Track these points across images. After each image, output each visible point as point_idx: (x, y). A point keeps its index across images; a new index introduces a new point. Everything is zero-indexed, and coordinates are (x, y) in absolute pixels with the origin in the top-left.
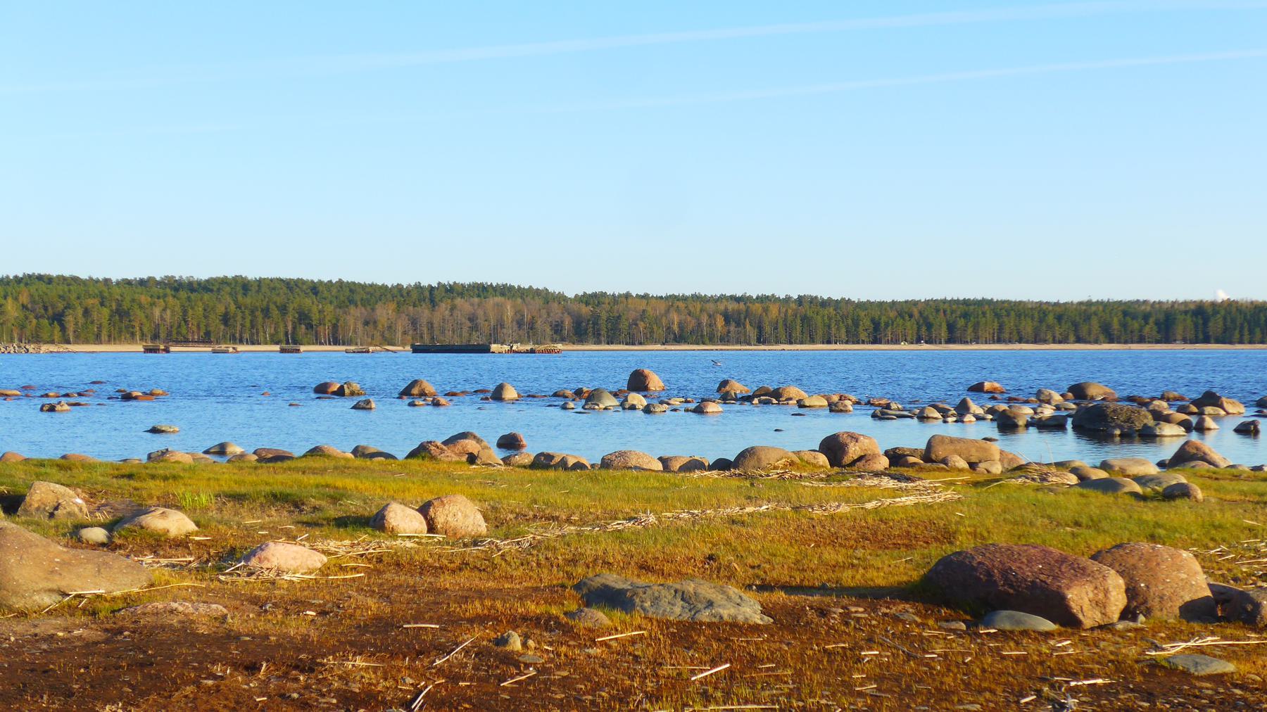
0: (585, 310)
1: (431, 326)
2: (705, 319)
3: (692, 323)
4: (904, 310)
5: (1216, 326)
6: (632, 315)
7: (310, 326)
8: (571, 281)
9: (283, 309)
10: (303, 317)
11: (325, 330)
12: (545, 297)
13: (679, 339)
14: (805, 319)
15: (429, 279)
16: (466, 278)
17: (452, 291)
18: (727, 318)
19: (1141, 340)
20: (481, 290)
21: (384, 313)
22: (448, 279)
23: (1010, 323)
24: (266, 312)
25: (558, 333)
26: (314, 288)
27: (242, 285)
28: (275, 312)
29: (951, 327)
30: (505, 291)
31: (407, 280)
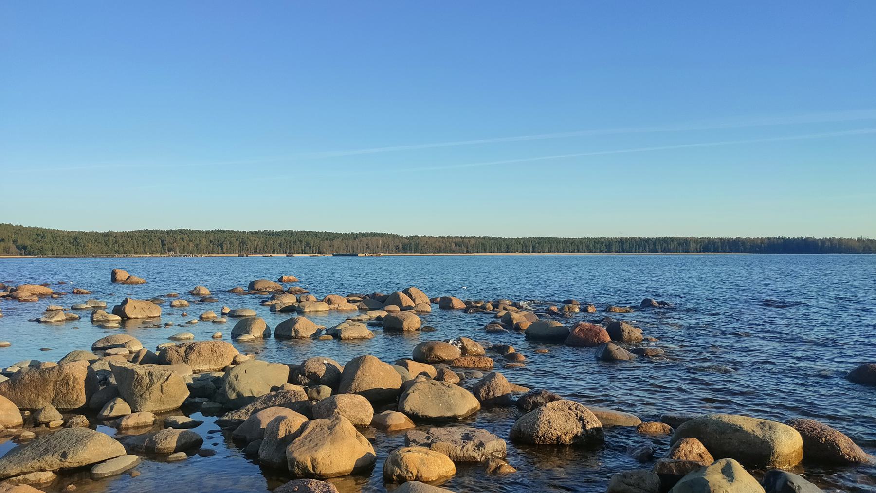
0: (407, 241)
1: (353, 247)
2: (448, 245)
3: (443, 246)
4: (518, 241)
5: (626, 246)
6: (423, 243)
9: (301, 242)
10: (308, 244)
11: (315, 249)
13: (439, 251)
14: (483, 244)
19: (600, 251)
21: (337, 243)
23: (554, 246)
24: (295, 242)
25: (397, 250)
28: (298, 243)
29: (534, 247)
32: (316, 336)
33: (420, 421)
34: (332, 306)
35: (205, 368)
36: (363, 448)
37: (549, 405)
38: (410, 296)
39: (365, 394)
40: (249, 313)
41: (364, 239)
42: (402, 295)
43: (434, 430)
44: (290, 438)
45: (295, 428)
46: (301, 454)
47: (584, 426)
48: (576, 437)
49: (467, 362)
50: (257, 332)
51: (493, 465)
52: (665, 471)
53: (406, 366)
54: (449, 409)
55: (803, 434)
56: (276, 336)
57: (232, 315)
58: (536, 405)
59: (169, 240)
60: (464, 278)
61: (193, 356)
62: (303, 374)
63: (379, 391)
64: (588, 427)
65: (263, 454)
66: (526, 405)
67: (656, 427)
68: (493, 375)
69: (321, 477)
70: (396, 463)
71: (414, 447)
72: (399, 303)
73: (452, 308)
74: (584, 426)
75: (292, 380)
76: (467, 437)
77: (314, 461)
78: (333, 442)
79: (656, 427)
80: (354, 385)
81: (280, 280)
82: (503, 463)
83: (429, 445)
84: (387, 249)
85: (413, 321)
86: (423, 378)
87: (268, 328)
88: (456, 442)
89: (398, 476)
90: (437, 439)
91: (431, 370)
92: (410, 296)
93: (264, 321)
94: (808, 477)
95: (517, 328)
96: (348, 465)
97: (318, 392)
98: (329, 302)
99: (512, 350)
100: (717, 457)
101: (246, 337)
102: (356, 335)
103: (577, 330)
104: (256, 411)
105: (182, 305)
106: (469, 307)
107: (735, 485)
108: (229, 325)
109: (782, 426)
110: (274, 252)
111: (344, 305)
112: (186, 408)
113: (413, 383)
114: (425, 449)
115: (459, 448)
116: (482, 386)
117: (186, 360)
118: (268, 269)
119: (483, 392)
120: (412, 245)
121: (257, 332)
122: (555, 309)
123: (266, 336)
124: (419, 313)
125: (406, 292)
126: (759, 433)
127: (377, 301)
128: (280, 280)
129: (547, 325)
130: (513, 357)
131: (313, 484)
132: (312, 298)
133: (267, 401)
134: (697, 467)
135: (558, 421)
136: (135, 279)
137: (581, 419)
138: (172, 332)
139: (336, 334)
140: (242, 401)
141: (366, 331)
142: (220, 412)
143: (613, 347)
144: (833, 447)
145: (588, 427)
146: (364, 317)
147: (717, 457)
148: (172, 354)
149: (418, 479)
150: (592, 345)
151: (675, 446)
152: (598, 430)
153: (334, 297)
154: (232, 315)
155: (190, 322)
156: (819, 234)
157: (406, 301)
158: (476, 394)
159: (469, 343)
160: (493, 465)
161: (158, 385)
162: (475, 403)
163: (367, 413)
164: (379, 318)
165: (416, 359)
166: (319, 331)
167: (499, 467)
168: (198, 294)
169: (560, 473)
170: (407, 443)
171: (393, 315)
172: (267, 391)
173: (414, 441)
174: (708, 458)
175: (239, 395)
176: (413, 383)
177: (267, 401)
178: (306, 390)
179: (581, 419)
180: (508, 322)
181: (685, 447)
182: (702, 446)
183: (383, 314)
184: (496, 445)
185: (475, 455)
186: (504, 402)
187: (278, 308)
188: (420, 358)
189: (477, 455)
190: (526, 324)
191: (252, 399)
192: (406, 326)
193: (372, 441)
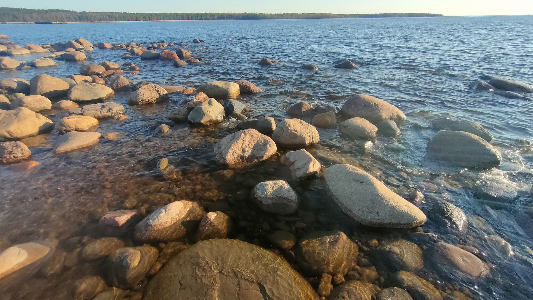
0: (80, 15)
7: (17, 18)
12: (72, 12)
13: (101, 20)
14: (123, 16)
15: (46, 8)
16: (54, 8)
18: (109, 16)
22: (50, 8)
25: (76, 20)
31: (40, 8)
32: (19, 68)
33: (81, 103)
34: (32, 51)
36: (44, 120)
38: (81, 44)
47: (160, 94)
48: (157, 99)
49: (109, 72)
52: (190, 107)
54: (96, 95)
55: (240, 86)
60: (112, 33)
64: (161, 94)
66: (135, 88)
70: (62, 125)
71: (73, 116)
72: (74, 47)
74: (160, 94)
77: (8, 132)
83: (82, 114)
84: (69, 19)
85: (81, 56)
88: (97, 110)
89: (66, 130)
91: (89, 78)
92: (81, 44)
95: (137, 55)
98: (29, 48)
99: (133, 65)
103: (163, 54)
106: (114, 47)
111: (40, 49)
116: (114, 83)
119: (114, 85)
120: (83, 17)
125: (77, 41)
126: (224, 87)
127: (61, 47)
129: (150, 53)
130: (133, 69)
134: (201, 103)
135: (148, 93)
139: (33, 65)
141: (52, 62)
145: (161, 94)
146: (53, 55)
152: (166, 95)
153: (32, 46)
157: (78, 46)
158: (111, 86)
160: (116, 117)
162: (110, 91)
163: (48, 104)
164: (61, 55)
165: (82, 74)
166: (22, 65)
167: (119, 117)
170: (70, 114)
171: (68, 53)
179: (158, 91)
180: (133, 52)
182: (205, 95)
184: (117, 108)
189: (109, 114)
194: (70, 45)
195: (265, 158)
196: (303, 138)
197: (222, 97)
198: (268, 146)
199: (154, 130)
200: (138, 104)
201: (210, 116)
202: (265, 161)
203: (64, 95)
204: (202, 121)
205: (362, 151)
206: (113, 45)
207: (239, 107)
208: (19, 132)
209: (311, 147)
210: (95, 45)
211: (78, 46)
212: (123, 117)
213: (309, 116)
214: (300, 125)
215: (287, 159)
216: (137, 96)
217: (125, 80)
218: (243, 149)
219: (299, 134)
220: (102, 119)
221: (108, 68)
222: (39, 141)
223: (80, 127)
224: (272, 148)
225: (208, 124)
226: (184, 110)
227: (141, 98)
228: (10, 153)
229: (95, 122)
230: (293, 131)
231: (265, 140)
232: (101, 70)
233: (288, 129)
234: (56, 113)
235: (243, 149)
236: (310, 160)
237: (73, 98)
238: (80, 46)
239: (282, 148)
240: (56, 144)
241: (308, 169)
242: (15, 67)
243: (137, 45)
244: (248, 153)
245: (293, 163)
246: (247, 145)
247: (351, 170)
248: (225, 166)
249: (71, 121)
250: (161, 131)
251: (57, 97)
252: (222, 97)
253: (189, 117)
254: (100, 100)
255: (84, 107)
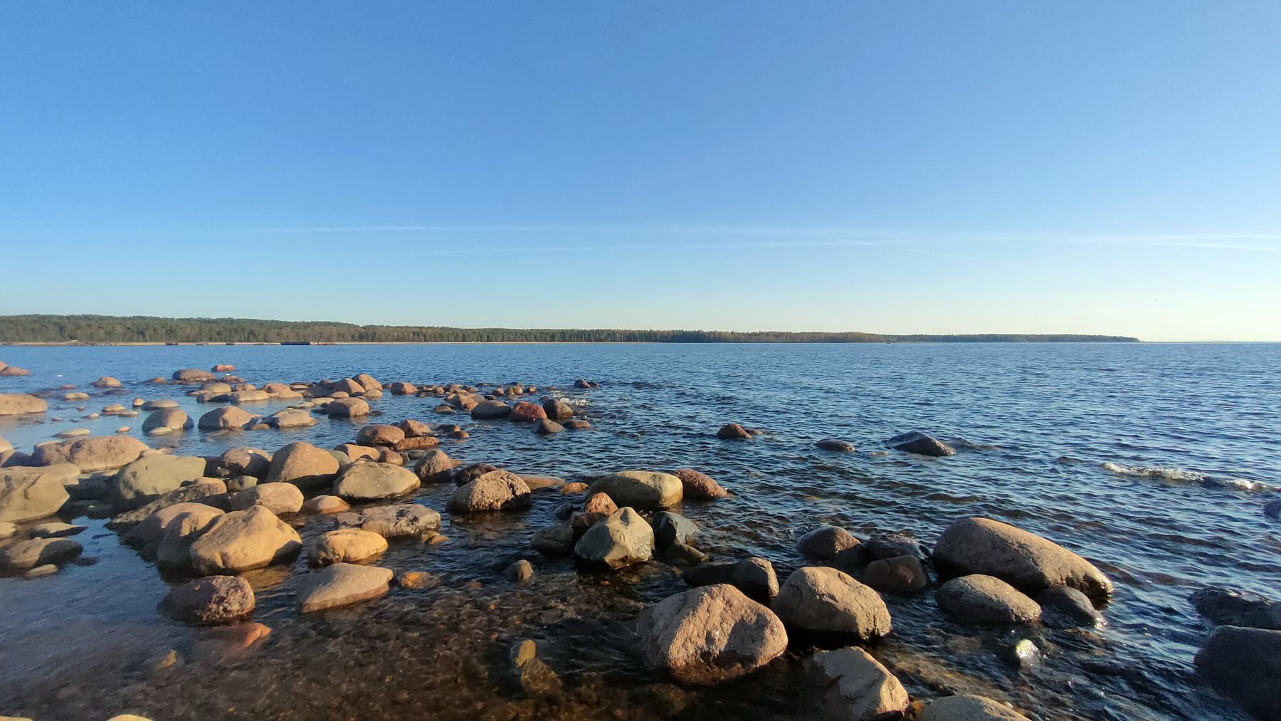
4: (474, 332)
5: (567, 337)
8: (362, 320)
10: (252, 333)
17: (315, 324)
20: (328, 324)
21: (285, 332)
25: (353, 338)
26: (261, 323)
27: (232, 321)
30: (336, 324)
32: (248, 427)
33: (355, 502)
35: (99, 466)
36: (289, 535)
37: (483, 476)
38: (361, 383)
39: (294, 482)
40: (167, 404)
41: (316, 328)
42: (350, 381)
43: (368, 511)
44: (196, 535)
45: (203, 523)
46: (208, 551)
47: (514, 493)
50: (175, 424)
51: (425, 537)
53: (345, 450)
54: (387, 488)
56: (200, 427)
57: (146, 407)
58: (474, 477)
59: (70, 327)
61: (81, 455)
62: (223, 466)
63: (313, 478)
64: (518, 493)
65: (162, 555)
66: (464, 477)
67: (576, 486)
68: (434, 453)
69: (236, 572)
70: (322, 547)
71: (343, 530)
73: (404, 393)
74: (514, 493)
75: (209, 472)
76: (401, 514)
78: (248, 534)
79: (576, 486)
80: (284, 473)
81: (215, 370)
82: (435, 534)
83: (360, 526)
84: (342, 337)
85: (360, 407)
86: (362, 462)
87: (189, 420)
89: (324, 560)
90: (371, 518)
91: (373, 452)
93: (182, 411)
94: (685, 514)
96: (268, 555)
97: (241, 483)
98: (269, 390)
99: (458, 429)
100: (619, 506)
101: (161, 431)
102: (295, 422)
104: (159, 508)
105: (79, 399)
106: (421, 391)
107: (630, 527)
108: (141, 417)
109: (668, 476)
110: (210, 340)
111: (287, 392)
112: (65, 514)
113: (350, 466)
114: (354, 530)
115: (392, 525)
116: (423, 464)
117: (71, 459)
118: (197, 359)
119: (423, 470)
120: (368, 334)
121: (175, 424)
122: (501, 391)
123: (188, 427)
124: (369, 399)
125: (356, 379)
126: (651, 484)
127: (326, 389)
128: (215, 370)
129: (492, 405)
130: (458, 436)
131: (219, 581)
132: (250, 387)
133: (174, 497)
134: (603, 517)
135: (491, 489)
136: (15, 370)
137: (511, 486)
138: (57, 428)
139: (273, 423)
140: (142, 500)
141: (306, 418)
142: (114, 514)
143: (548, 422)
144: (703, 489)
145: (518, 493)
146: (308, 404)
147: (619, 506)
148: (51, 454)
149: (346, 560)
150: (529, 421)
151: (588, 500)
152: (527, 494)
154: (146, 407)
155: (87, 417)
156: (706, 328)
157: (356, 387)
159: (414, 425)
160: (425, 537)
161: (20, 490)
162: (414, 480)
163: (296, 500)
164: (324, 405)
165: (360, 444)
166: (253, 421)
167: (431, 539)
168: (105, 386)
169: (489, 535)
170: (337, 525)
172: (175, 486)
173: (344, 523)
174: (614, 507)
175: (138, 493)
176: (350, 466)
177: (174, 497)
178: (226, 482)
179: (511, 486)
180: (457, 404)
181: (595, 501)
183: (329, 401)
184: (429, 517)
185: (409, 529)
186: (444, 478)
187: (207, 398)
188: (364, 441)
189: (411, 530)
190: (473, 405)
191: (155, 498)
192: (352, 411)
193: (297, 528)
194: (343, 386)
195: (762, 661)
196: (850, 620)
197: (649, 504)
198: (768, 632)
199: (503, 570)
200: (468, 512)
201: (624, 547)
202: (762, 668)
203: (327, 484)
204: (607, 559)
205: (1012, 663)
206: (420, 388)
207: (685, 528)
208: (242, 556)
209: (875, 642)
210: (384, 387)
211: (356, 387)
212: (438, 537)
213: (861, 563)
214: (840, 583)
215: (819, 669)
216: (470, 492)
217: (443, 461)
218: (709, 633)
219: (840, 606)
220: (396, 540)
221: (409, 433)
222: (275, 578)
223: (354, 554)
224: (777, 638)
225: (619, 565)
226: (566, 529)
227: (476, 498)
228: (222, 600)
229: (381, 544)
230: (826, 599)
231: (759, 615)
232: (397, 436)
233: (814, 593)
234: (309, 520)
235: (709, 633)
236: (880, 678)
237: (342, 492)
238: (359, 389)
239: (800, 639)
240: (307, 587)
241: (877, 701)
242: (241, 424)
243: (465, 388)
244: (721, 643)
245: (834, 683)
246: (717, 624)
247: (997, 715)
248: (666, 674)
249: (341, 540)
250: (516, 577)
251: (314, 486)
252: (649, 504)
253: (577, 548)
254: (392, 499)
255: (365, 511)
